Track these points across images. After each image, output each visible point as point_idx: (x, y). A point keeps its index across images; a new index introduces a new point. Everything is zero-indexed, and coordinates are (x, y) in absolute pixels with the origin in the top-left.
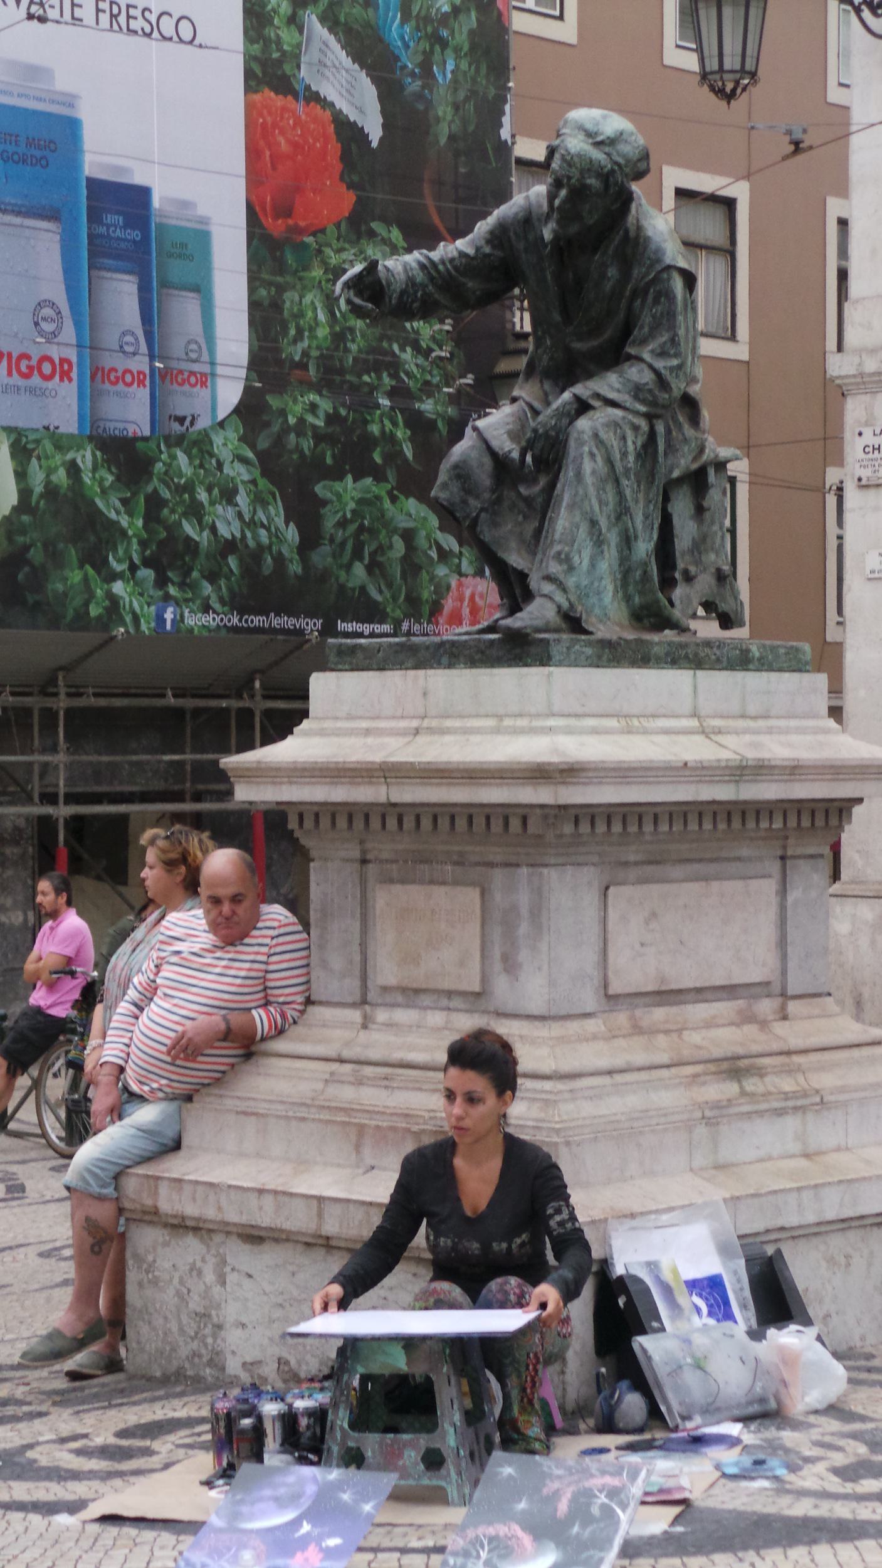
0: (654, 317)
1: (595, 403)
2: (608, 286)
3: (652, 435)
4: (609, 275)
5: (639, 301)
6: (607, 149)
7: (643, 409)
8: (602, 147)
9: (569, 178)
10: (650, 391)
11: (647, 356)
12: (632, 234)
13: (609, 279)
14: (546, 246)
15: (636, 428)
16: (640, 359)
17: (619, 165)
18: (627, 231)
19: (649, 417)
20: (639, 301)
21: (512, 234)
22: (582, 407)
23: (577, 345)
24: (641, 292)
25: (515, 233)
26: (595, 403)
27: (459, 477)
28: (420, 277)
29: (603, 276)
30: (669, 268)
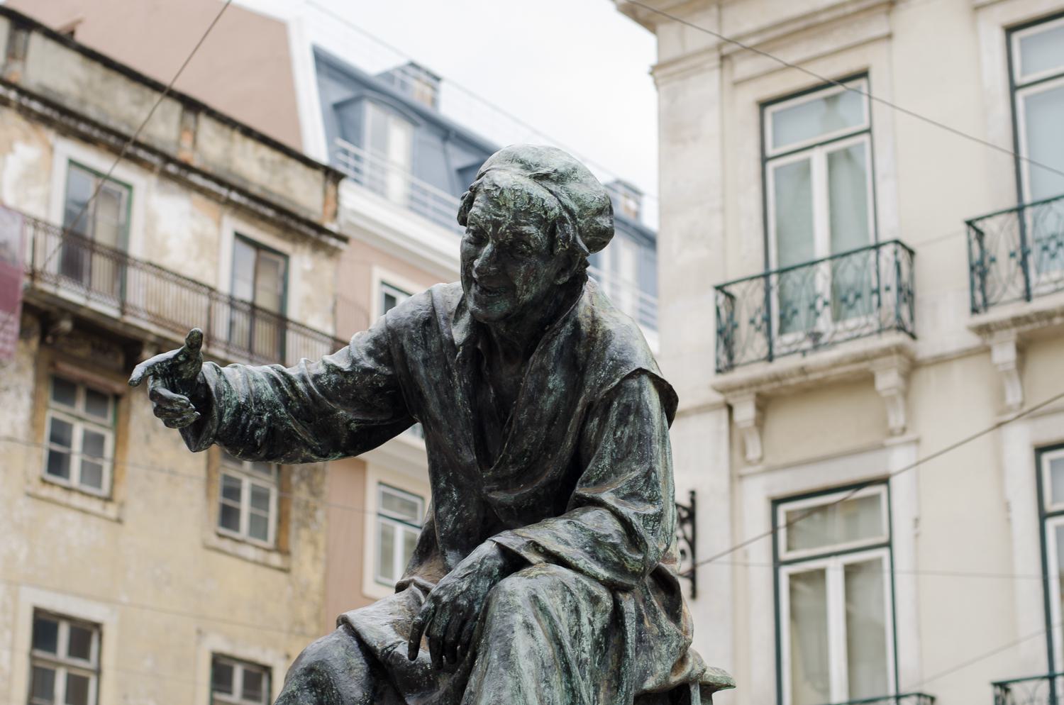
0: (618, 442)
1: (533, 558)
2: (548, 402)
3: (617, 615)
4: (551, 386)
5: (596, 421)
6: (553, 187)
7: (604, 573)
8: (545, 183)
9: (497, 224)
10: (614, 546)
11: (607, 497)
12: (585, 328)
13: (550, 392)
14: (456, 350)
15: (594, 600)
16: (600, 504)
17: (571, 212)
18: (577, 324)
19: (614, 588)
20: (596, 421)
21: (405, 341)
22: (513, 563)
23: (499, 496)
24: (598, 408)
25: (411, 340)
26: (533, 558)
27: (313, 685)
28: (268, 392)
29: (541, 388)
30: (641, 372)
